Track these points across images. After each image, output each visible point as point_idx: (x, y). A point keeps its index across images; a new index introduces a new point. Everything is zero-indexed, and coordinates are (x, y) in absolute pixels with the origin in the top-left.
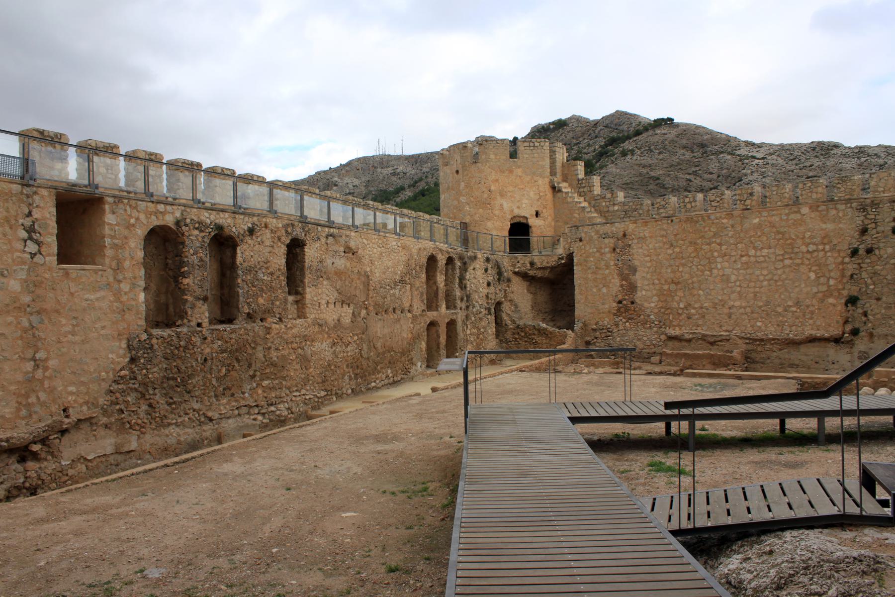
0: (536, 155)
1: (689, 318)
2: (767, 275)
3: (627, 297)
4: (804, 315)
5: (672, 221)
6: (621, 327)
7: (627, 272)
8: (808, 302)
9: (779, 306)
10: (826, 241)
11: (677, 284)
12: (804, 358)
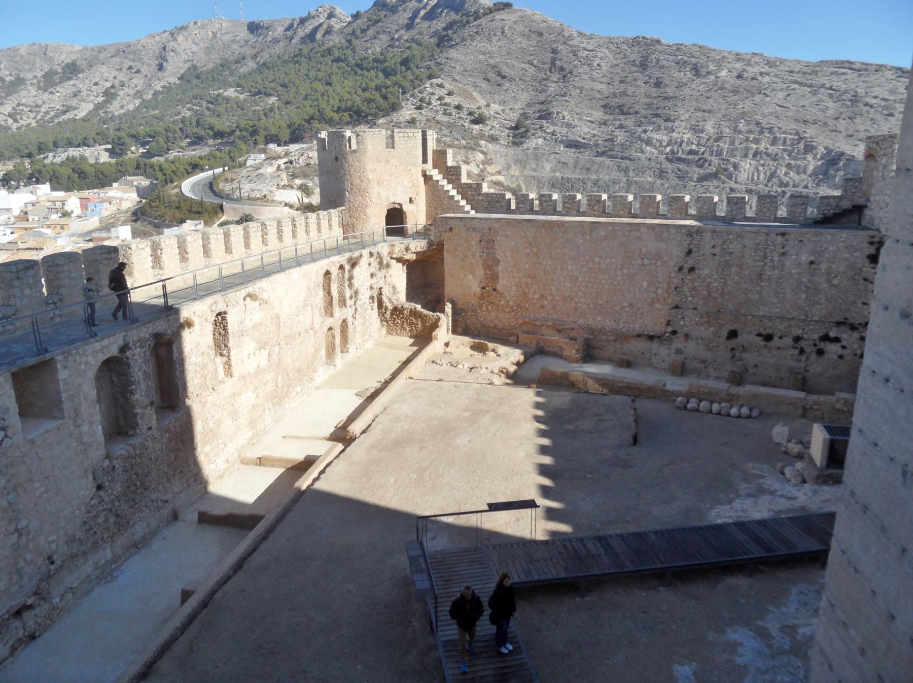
0: (410, 145)
1: (542, 307)
6: (484, 309)
7: (490, 263)
11: (534, 278)
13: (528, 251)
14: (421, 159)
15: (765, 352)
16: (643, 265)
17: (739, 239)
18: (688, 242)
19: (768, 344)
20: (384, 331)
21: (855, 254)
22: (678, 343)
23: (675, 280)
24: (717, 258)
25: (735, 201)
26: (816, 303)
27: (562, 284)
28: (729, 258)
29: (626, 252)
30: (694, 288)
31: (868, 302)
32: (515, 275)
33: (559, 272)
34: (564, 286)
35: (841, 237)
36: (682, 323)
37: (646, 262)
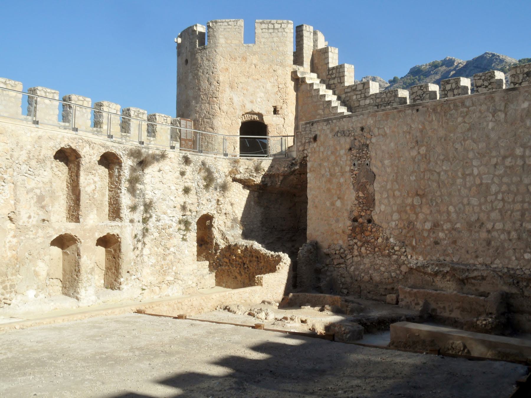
0: (275, 39)
1: (436, 243)
3: (363, 214)
5: (418, 110)
6: (356, 253)
7: (364, 180)
11: (422, 196)
13: (414, 153)
14: (292, 58)
20: (211, 279)
27: (465, 201)
32: (397, 193)
33: (459, 181)
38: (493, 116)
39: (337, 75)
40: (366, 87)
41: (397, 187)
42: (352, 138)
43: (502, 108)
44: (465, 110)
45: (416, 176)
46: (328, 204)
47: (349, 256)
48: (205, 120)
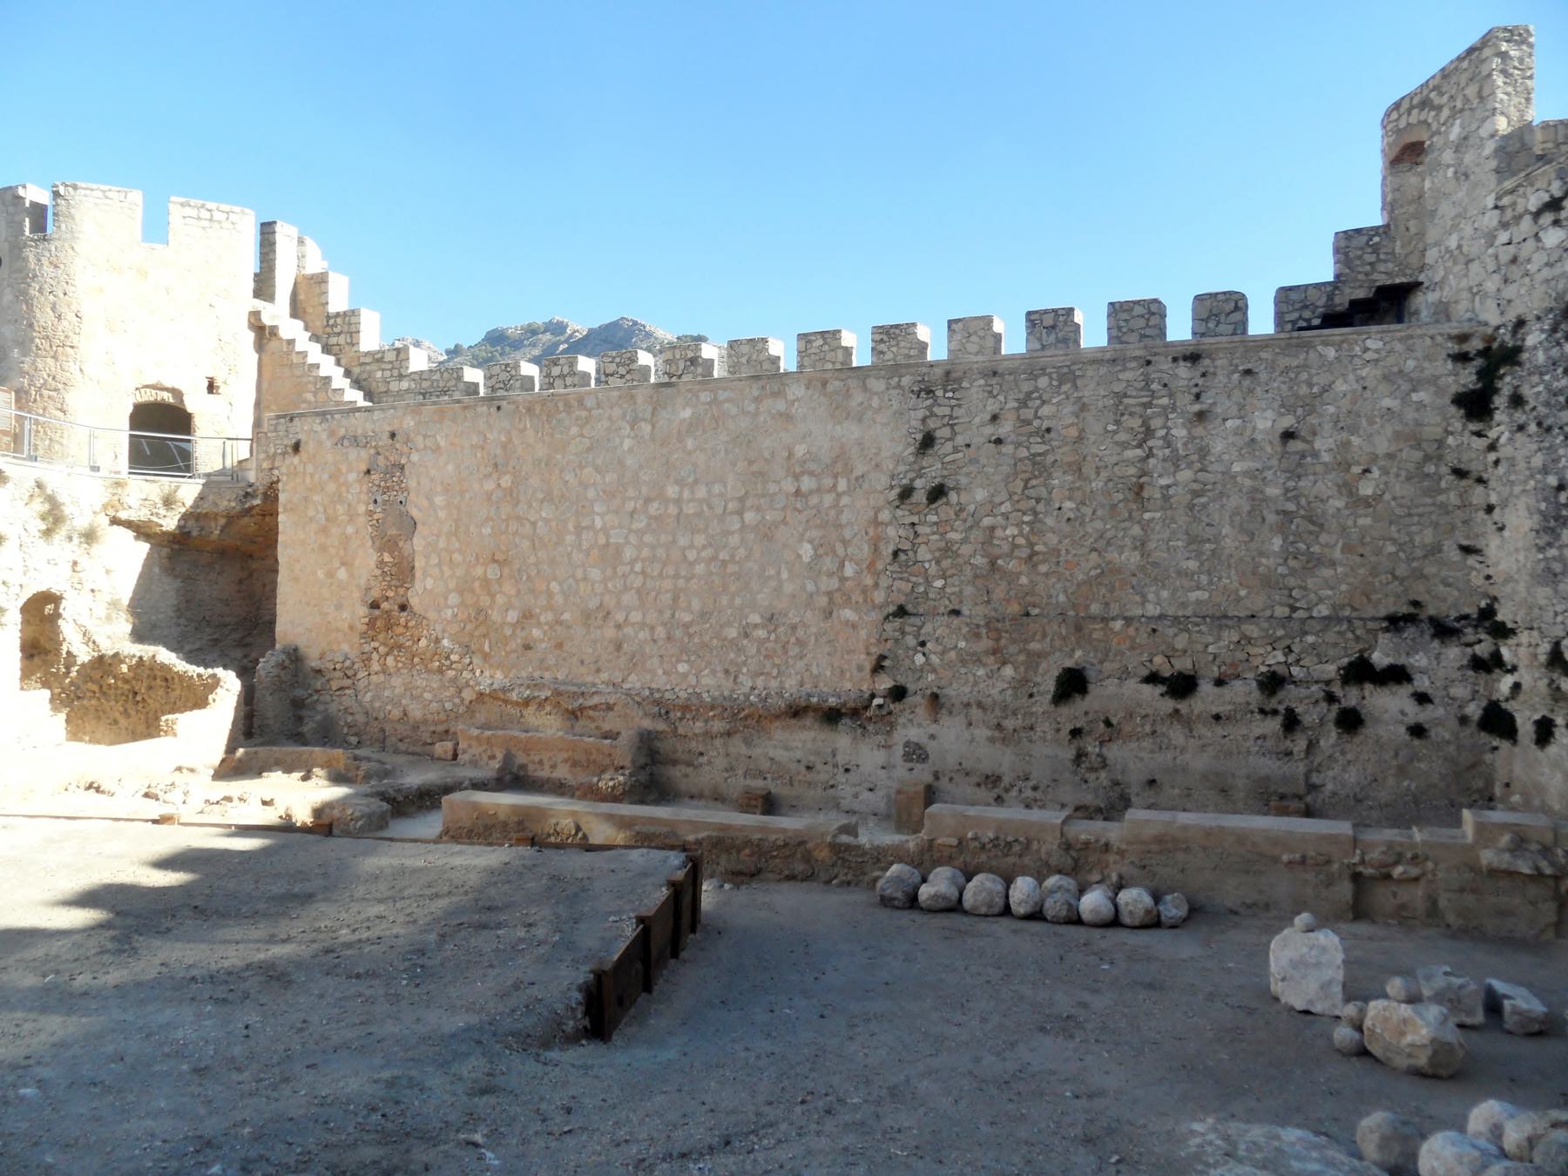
1: (527, 647)
2: (704, 547)
3: (391, 594)
4: (785, 652)
5: (499, 408)
6: (376, 667)
7: (393, 532)
8: (793, 617)
9: (729, 624)
10: (839, 467)
11: (501, 564)
12: (780, 754)
13: (490, 485)
14: (250, 285)
15: (1177, 735)
16: (798, 493)
17: (1065, 388)
18: (921, 414)
19: (1183, 706)
21: (1415, 397)
22: (913, 727)
23: (891, 531)
24: (1007, 449)
25: (1048, 321)
26: (1315, 562)
27: (579, 573)
28: (1040, 449)
29: (750, 463)
30: (948, 550)
31: (1480, 544)
32: (457, 557)
33: (570, 539)
34: (585, 579)
35: (1366, 350)
36: (919, 659)
37: (807, 483)
38: (632, 429)
39: (346, 328)
40: (402, 356)
41: (457, 545)
42: (372, 451)
43: (648, 415)
44: (584, 414)
45: (492, 528)
46: (321, 574)
47: (361, 674)
48: (45, 393)
